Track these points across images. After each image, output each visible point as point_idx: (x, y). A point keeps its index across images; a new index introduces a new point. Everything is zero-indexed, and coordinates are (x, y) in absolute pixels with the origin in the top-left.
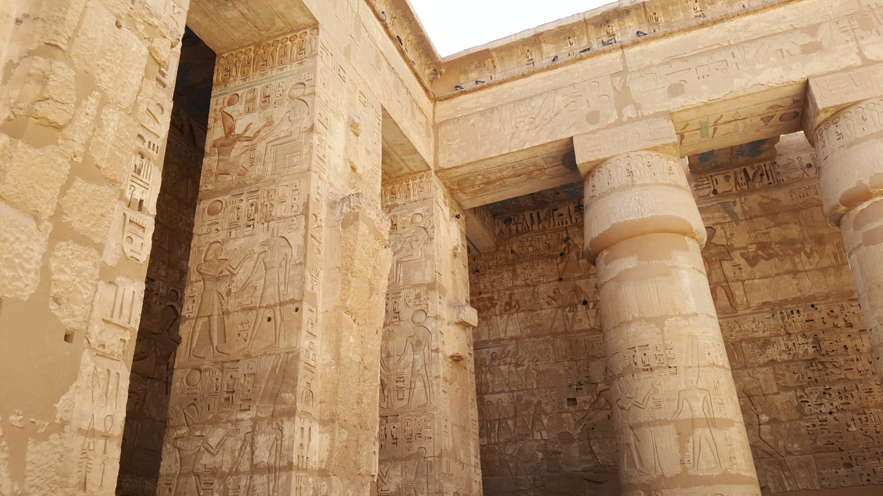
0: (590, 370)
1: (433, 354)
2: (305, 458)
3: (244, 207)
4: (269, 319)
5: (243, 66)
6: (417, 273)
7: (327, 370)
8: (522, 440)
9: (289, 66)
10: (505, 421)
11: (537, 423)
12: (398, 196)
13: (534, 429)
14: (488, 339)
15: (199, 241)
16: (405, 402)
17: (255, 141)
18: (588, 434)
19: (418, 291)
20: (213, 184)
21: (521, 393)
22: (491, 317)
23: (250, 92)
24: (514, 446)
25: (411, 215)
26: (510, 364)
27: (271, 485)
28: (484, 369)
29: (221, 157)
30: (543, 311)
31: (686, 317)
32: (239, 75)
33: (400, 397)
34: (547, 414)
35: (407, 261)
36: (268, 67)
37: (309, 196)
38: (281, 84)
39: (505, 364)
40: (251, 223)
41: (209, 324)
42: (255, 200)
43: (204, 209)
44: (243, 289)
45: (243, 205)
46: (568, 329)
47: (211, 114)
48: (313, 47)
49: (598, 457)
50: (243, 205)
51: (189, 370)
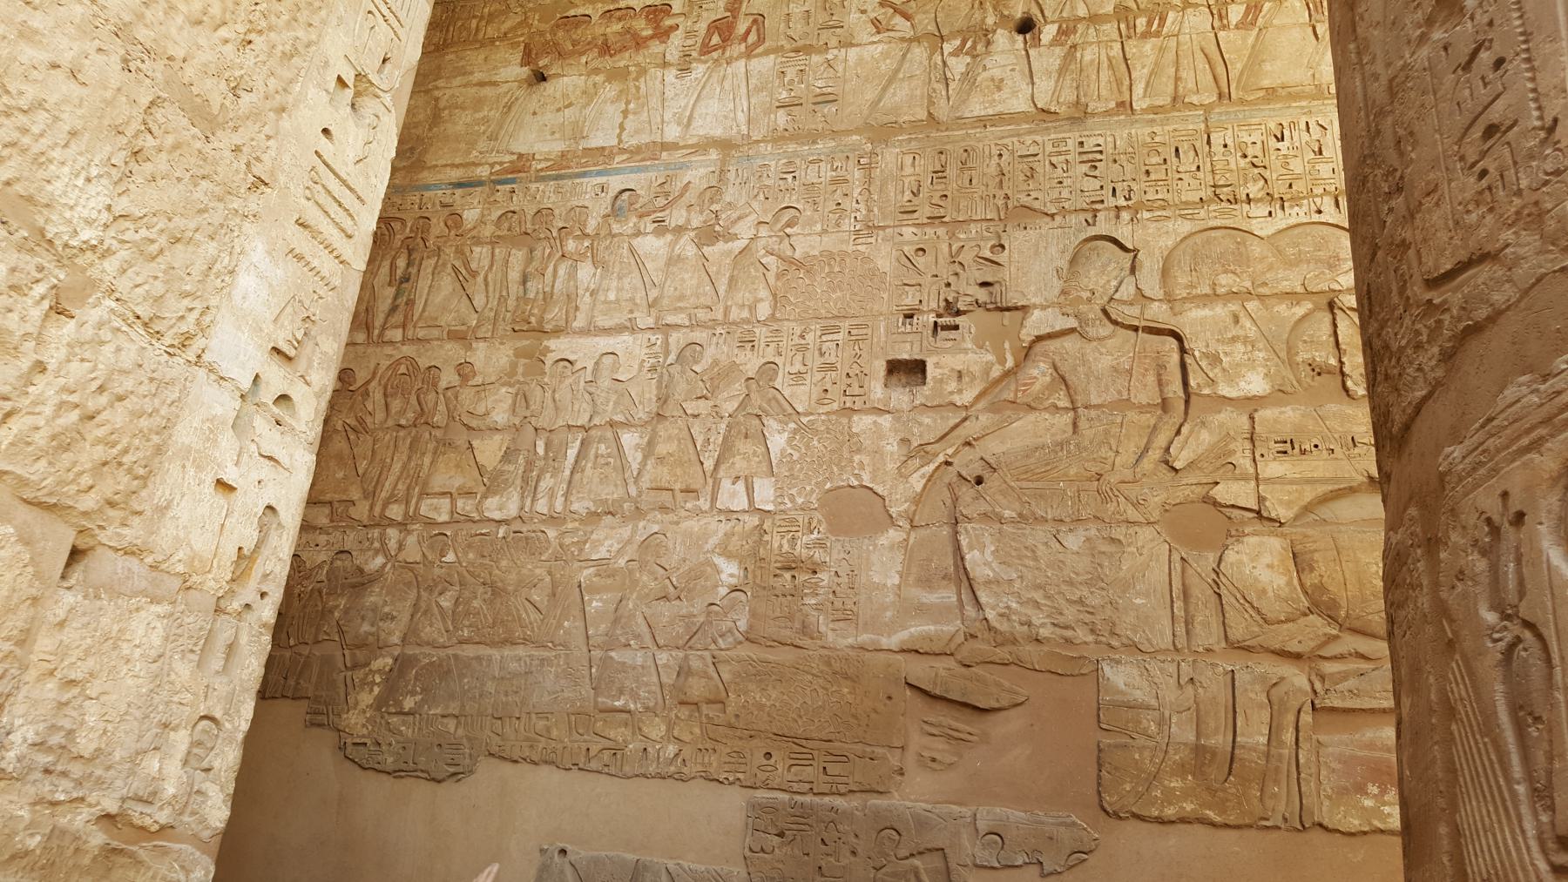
0: (1002, 258)
8: (664, 509)
10: (609, 434)
11: (743, 446)
13: (723, 467)
14: (615, 142)
18: (955, 500)
21: (699, 336)
22: (642, 72)
24: (626, 532)
26: (679, 230)
28: (571, 245)
30: (853, 53)
34: (789, 413)
39: (661, 228)
46: (942, 111)
49: (983, 599)
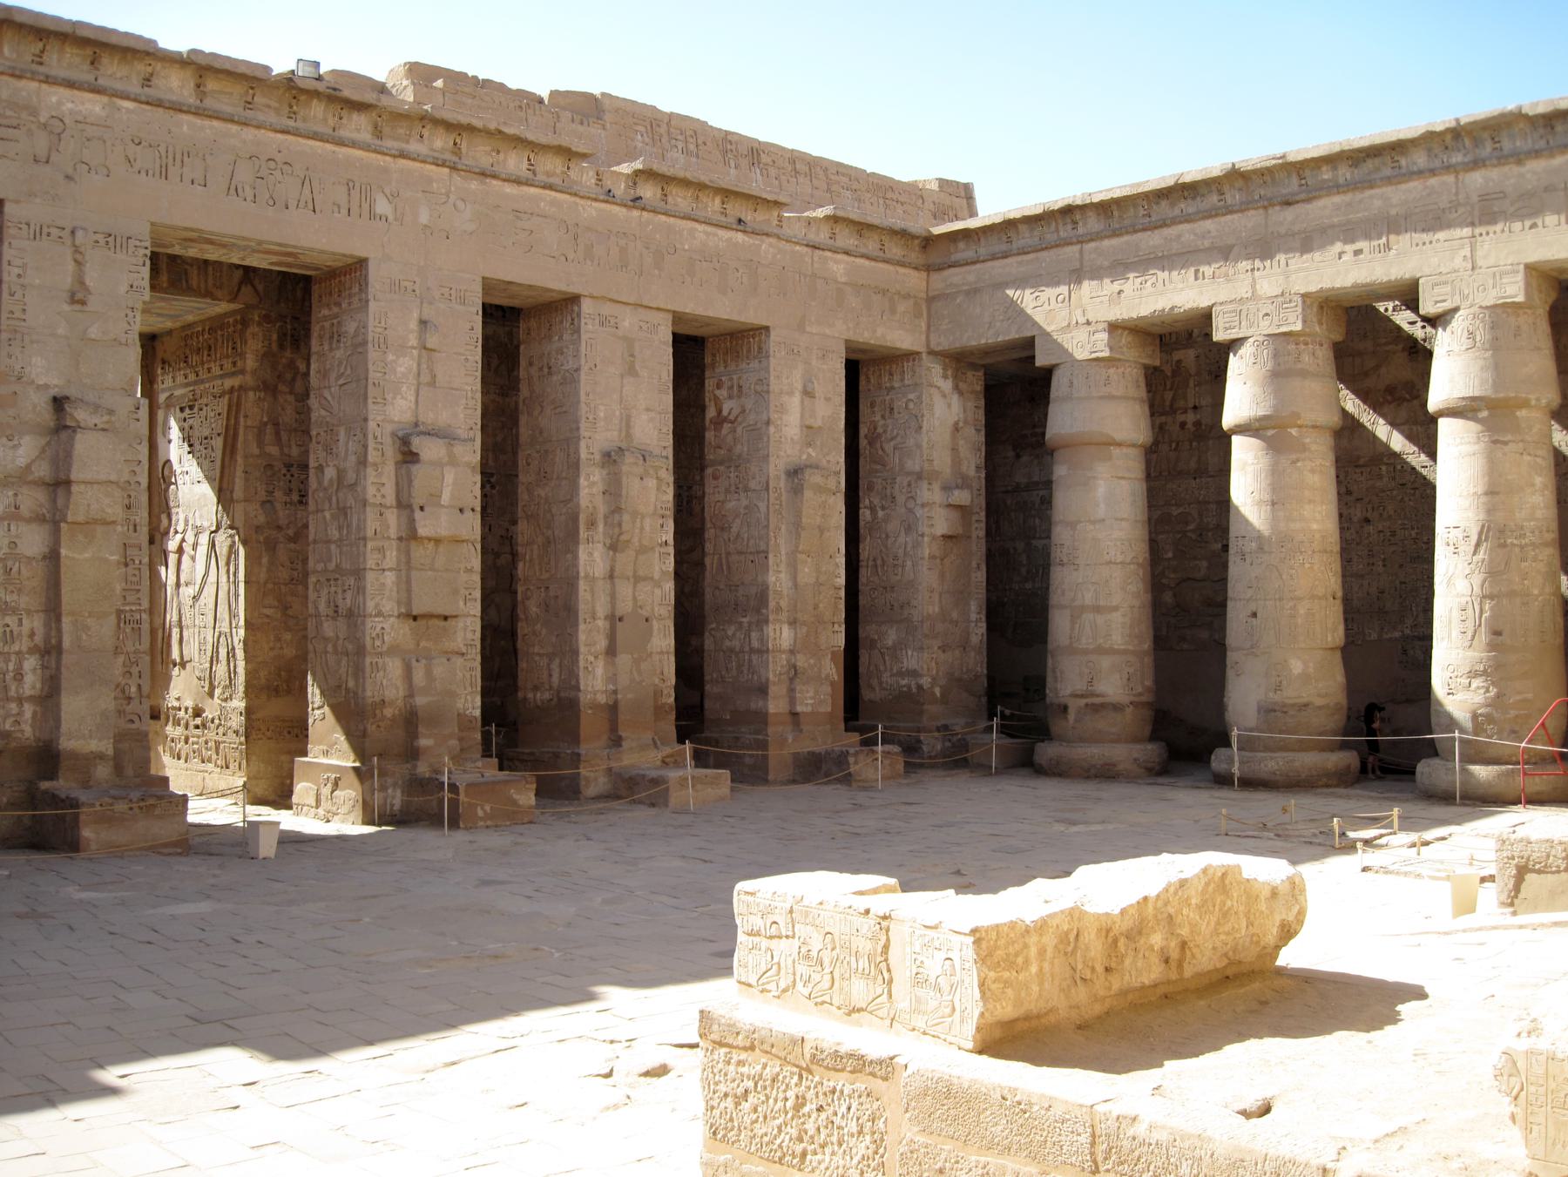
16: (899, 578)
19: (909, 479)
25: (904, 400)
31: (1093, 522)
41: (720, 559)
45: (732, 475)
50: (732, 475)
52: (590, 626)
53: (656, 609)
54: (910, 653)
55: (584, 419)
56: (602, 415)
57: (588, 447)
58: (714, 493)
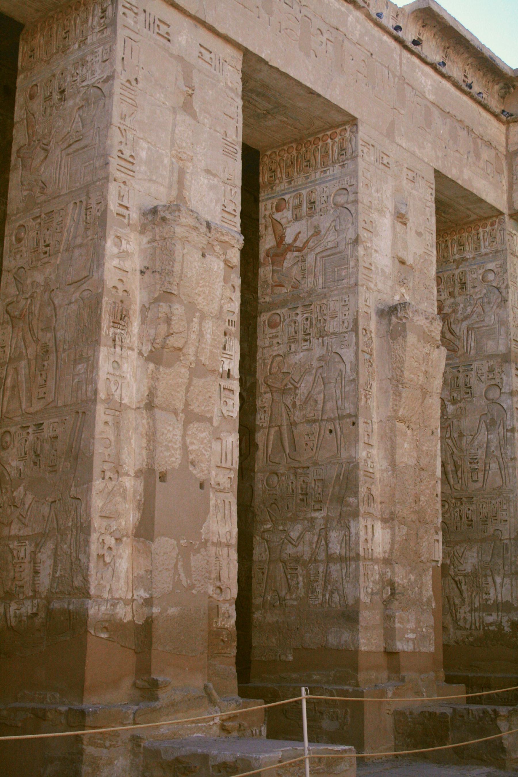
1: (509, 434)
2: (370, 550)
3: (300, 321)
4: (331, 431)
5: (288, 167)
6: (490, 343)
7: (385, 475)
9: (331, 169)
12: (467, 248)
15: (263, 354)
16: (479, 485)
17: (305, 251)
19: (491, 363)
20: (270, 297)
23: (295, 197)
25: (481, 271)
27: (344, 571)
29: (275, 268)
32: (284, 177)
33: (474, 479)
35: (478, 328)
36: (311, 168)
37: (357, 312)
38: (325, 190)
40: (307, 337)
41: (280, 433)
42: (309, 315)
43: (264, 322)
44: (306, 402)
45: (299, 318)
47: (262, 221)
48: (354, 146)
50: (299, 318)
51: (268, 474)
52: (110, 485)
53: (213, 473)
54: (498, 580)
55: (115, 153)
56: (143, 154)
57: (121, 197)
58: (271, 346)
